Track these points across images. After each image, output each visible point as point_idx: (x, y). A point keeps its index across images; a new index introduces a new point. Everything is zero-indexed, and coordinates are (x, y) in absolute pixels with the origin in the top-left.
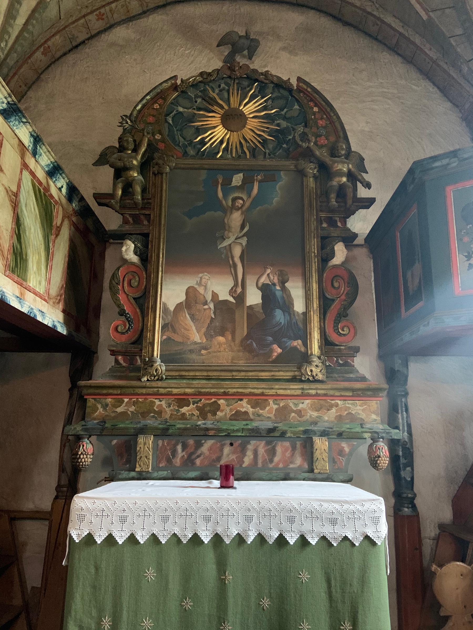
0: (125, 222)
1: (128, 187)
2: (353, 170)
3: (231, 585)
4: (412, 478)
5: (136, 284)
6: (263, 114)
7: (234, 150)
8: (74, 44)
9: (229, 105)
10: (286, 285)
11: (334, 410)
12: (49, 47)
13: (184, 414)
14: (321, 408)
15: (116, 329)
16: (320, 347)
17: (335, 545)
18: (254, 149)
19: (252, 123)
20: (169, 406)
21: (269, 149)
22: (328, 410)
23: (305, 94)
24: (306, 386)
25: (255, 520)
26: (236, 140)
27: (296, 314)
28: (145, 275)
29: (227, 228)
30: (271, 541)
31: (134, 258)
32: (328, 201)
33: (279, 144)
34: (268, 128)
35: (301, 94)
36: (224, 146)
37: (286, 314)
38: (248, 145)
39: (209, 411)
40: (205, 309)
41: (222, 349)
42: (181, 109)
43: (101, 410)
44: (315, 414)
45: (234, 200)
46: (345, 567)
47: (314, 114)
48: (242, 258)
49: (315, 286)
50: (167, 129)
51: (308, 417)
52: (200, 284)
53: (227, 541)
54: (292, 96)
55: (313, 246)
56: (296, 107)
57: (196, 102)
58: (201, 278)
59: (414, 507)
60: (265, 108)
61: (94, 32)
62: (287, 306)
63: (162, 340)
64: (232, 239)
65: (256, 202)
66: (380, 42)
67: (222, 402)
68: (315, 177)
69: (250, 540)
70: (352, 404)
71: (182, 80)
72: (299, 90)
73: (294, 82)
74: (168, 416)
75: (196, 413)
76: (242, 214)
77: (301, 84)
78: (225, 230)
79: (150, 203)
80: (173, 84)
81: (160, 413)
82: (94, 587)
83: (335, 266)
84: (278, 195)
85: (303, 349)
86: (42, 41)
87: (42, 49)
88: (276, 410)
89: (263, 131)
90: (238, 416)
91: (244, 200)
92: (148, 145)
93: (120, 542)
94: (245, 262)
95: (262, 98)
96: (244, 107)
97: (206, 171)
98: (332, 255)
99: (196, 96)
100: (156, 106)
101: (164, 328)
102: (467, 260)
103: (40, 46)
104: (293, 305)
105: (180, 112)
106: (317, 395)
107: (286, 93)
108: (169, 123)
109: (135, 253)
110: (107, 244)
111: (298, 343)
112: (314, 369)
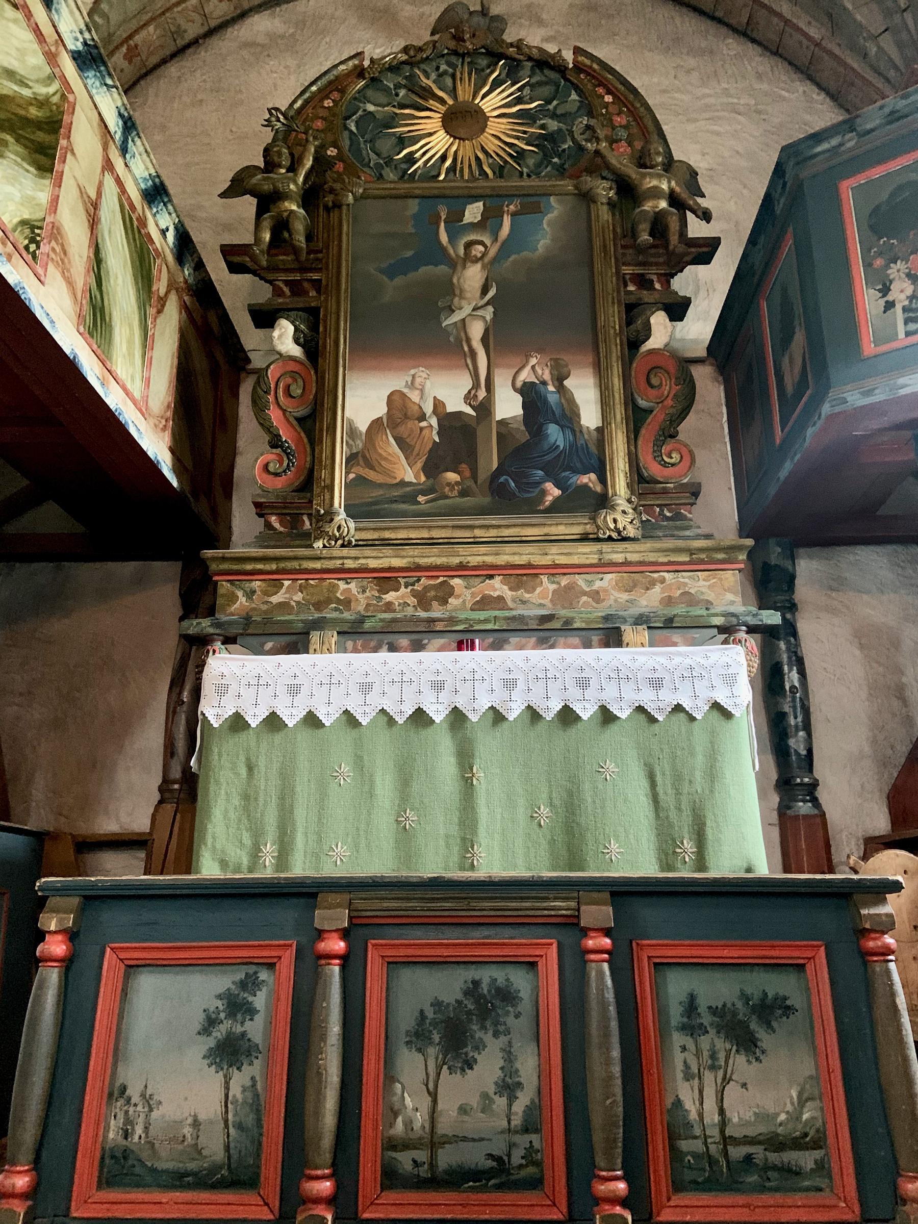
0: (278, 292)
1: (281, 226)
2: (678, 189)
3: (484, 786)
4: (810, 751)
5: (299, 391)
6: (514, 109)
7: (466, 171)
8: (181, 43)
9: (455, 98)
10: (565, 382)
11: (658, 588)
12: (136, 46)
13: (389, 604)
14: (635, 586)
15: (266, 468)
16: (630, 486)
17: (660, 719)
18: (502, 168)
19: (496, 126)
20: (364, 591)
21: (528, 167)
22: (648, 589)
23: (588, 74)
24: (606, 547)
25: (521, 685)
26: (470, 153)
27: (585, 430)
28: (314, 378)
29: (457, 292)
30: (549, 716)
31: (296, 351)
32: (634, 235)
33: (546, 158)
34: (525, 132)
35: (582, 76)
36: (448, 163)
37: (568, 432)
38: (491, 161)
39: (436, 598)
40: (422, 429)
41: (456, 493)
42: (371, 108)
43: (242, 599)
44: (625, 596)
45: (469, 245)
46: (679, 753)
47: (606, 105)
48: (485, 340)
49: (617, 383)
50: (347, 142)
51: (612, 602)
52: (412, 385)
53: (474, 718)
54: (566, 80)
55: (612, 317)
56: (574, 96)
57: (397, 95)
58: (414, 376)
59: (815, 801)
60: (519, 101)
61: (213, 23)
62: (568, 417)
63: (348, 481)
64: (467, 309)
65: (506, 249)
66: (720, 21)
67: (456, 582)
68: (611, 204)
69: (511, 717)
70: (690, 577)
71: (372, 60)
72: (578, 68)
73: (568, 56)
74: (361, 608)
75: (412, 601)
76: (483, 267)
77: (580, 59)
78: (455, 295)
79: (320, 260)
80: (355, 67)
81: (347, 603)
82: (246, 797)
83: (652, 352)
84: (547, 232)
85: (599, 489)
86: (125, 36)
87: (124, 49)
88: (554, 591)
89: (518, 138)
90: (485, 602)
91: (487, 244)
92: (316, 159)
93: (291, 723)
94: (492, 346)
95: (513, 84)
96: (482, 99)
97: (417, 201)
98: (647, 332)
99: (398, 86)
100: (328, 103)
101: (351, 460)
102: (883, 296)
103: (122, 44)
104: (579, 416)
105: (370, 112)
106: (626, 563)
107: (553, 75)
108: (351, 131)
109: (296, 341)
110: (243, 375)
111: (589, 479)
112: (619, 517)
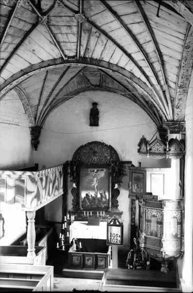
98: (115, 186)
109: (76, 185)
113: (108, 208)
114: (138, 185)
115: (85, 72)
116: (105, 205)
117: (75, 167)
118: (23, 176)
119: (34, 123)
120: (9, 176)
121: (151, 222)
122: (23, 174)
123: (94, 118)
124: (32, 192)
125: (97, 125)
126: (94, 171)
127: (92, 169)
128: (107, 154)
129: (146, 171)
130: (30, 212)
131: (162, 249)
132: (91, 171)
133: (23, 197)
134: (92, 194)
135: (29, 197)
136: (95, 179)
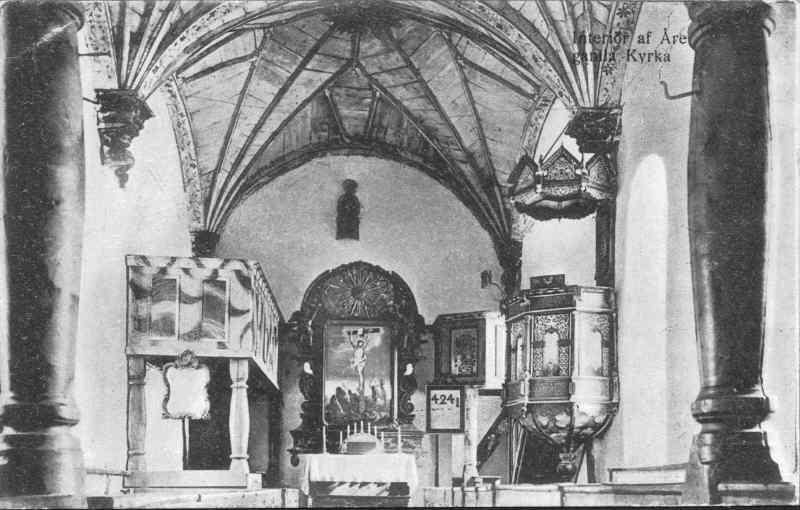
45: (359, 342)
48: (363, 372)
98: (405, 370)
113: (390, 420)
114: (463, 358)
115: (337, 90)
116: (383, 414)
117: (310, 323)
118: (221, 272)
119: (202, 220)
120: (186, 271)
121: (543, 347)
122: (222, 266)
123: (348, 221)
124: (242, 313)
125: (356, 237)
126: (355, 332)
127: (352, 329)
128: (386, 293)
129: (484, 320)
130: (237, 359)
131: (573, 396)
132: (349, 333)
133: (219, 323)
134: (351, 386)
135: (236, 325)
136: (359, 352)
